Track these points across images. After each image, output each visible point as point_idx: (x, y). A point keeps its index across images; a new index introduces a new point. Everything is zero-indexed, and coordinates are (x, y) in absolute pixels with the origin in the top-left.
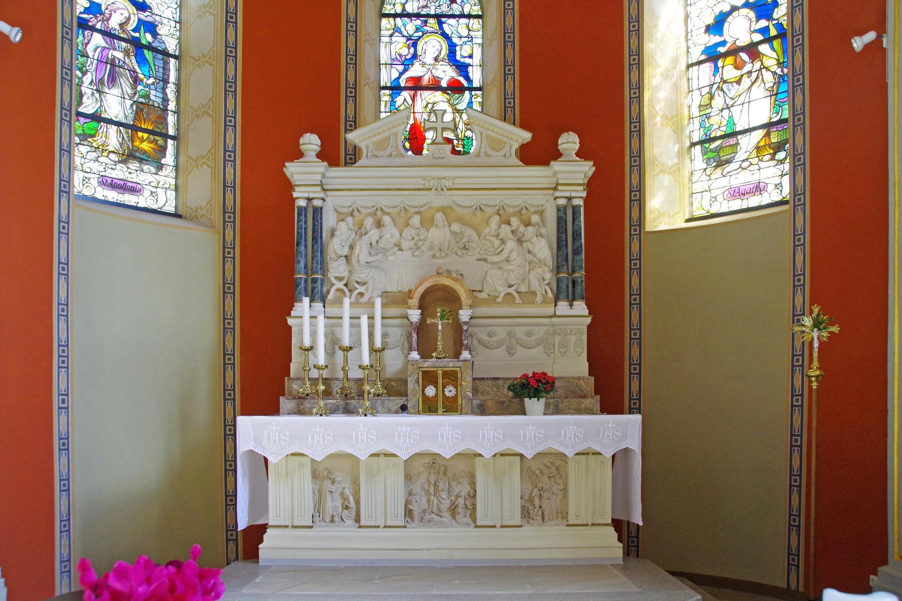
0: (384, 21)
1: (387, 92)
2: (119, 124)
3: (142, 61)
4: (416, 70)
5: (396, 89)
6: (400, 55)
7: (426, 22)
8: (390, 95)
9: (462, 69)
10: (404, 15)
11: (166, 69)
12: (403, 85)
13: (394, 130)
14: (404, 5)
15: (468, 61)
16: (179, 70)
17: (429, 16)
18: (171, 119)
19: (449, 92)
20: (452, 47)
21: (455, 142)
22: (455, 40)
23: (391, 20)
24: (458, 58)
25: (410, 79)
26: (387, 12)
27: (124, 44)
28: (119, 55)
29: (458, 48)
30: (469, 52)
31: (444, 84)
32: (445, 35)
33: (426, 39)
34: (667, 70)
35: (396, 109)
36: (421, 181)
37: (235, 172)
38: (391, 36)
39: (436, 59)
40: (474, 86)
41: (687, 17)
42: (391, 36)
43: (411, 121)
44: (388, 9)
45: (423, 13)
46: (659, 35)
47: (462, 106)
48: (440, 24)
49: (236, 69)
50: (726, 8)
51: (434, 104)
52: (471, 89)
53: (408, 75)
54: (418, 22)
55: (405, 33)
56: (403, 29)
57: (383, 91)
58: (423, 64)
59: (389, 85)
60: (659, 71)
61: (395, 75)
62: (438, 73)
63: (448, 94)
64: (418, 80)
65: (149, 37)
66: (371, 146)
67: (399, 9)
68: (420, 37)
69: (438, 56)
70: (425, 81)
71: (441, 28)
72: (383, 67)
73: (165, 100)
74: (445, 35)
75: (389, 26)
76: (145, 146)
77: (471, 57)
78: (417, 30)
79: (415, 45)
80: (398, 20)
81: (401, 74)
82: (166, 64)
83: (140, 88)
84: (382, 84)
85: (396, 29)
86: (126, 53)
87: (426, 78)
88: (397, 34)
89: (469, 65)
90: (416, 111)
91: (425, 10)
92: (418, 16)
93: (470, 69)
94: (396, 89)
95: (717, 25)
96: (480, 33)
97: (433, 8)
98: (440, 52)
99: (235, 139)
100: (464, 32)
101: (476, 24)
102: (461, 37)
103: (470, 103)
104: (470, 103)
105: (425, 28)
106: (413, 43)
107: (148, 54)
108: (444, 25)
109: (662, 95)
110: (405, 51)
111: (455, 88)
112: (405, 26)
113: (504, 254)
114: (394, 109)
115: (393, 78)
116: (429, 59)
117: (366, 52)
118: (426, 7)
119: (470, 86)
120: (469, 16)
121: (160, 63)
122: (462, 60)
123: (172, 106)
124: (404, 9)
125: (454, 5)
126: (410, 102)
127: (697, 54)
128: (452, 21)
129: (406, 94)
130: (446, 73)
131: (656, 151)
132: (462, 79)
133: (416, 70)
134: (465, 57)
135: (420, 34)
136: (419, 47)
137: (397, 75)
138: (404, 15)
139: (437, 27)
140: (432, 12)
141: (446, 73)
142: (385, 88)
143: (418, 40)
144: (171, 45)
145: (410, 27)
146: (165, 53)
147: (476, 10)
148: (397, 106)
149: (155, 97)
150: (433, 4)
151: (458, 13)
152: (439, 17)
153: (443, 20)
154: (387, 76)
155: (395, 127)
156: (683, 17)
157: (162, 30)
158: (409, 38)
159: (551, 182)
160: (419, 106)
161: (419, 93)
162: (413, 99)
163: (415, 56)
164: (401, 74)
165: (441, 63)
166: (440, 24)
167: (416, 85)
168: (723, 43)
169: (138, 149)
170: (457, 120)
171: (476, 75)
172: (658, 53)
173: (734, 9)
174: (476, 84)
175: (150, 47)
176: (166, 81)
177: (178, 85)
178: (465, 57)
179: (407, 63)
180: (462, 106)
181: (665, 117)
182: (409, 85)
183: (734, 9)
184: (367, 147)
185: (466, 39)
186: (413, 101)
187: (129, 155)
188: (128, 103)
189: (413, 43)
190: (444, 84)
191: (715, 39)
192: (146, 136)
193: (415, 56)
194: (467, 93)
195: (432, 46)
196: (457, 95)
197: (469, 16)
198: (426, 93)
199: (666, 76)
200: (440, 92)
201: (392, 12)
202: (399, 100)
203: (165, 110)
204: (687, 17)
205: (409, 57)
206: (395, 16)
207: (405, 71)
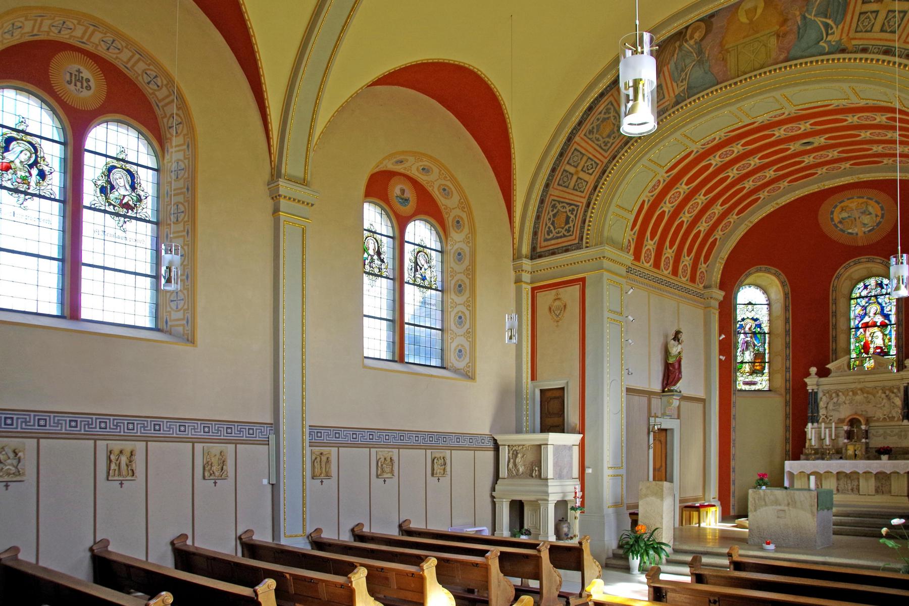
0: (852, 302)
3: (756, 338)
4: (866, 319)
5: (857, 328)
7: (870, 299)
9: (887, 316)
10: (861, 297)
11: (765, 339)
12: (860, 326)
15: (889, 313)
17: (871, 296)
18: (767, 356)
20: (882, 308)
22: (884, 305)
23: (855, 300)
24: (885, 312)
27: (750, 335)
28: (749, 339)
31: (878, 324)
39: (875, 314)
43: (864, 341)
52: (891, 325)
53: (862, 322)
54: (867, 299)
58: (870, 317)
61: (857, 322)
64: (867, 323)
65: (759, 329)
72: (852, 321)
73: (765, 350)
77: (891, 311)
78: (867, 303)
79: (865, 309)
81: (859, 322)
82: (765, 337)
83: (756, 348)
84: (851, 327)
85: (857, 304)
86: (751, 337)
93: (890, 316)
94: (857, 328)
103: (891, 331)
104: (891, 331)
106: (864, 308)
107: (759, 336)
110: (861, 313)
111: (883, 326)
113: (883, 404)
116: (871, 314)
118: (870, 292)
121: (763, 337)
123: (767, 351)
124: (860, 295)
126: (863, 333)
129: (861, 330)
130: (879, 319)
133: (866, 319)
135: (867, 304)
136: (868, 310)
138: (861, 297)
139: (875, 300)
141: (879, 319)
144: (766, 330)
145: (863, 302)
146: (765, 333)
149: (761, 349)
157: (763, 326)
158: (863, 307)
159: (900, 377)
160: (868, 333)
163: (866, 314)
164: (859, 322)
167: (866, 326)
174: (893, 322)
175: (759, 333)
176: (765, 343)
177: (769, 343)
179: (862, 317)
180: (887, 332)
188: (752, 354)
189: (864, 308)
190: (878, 324)
194: (889, 326)
195: (873, 309)
202: (858, 333)
203: (765, 353)
206: (857, 298)
207: (861, 320)
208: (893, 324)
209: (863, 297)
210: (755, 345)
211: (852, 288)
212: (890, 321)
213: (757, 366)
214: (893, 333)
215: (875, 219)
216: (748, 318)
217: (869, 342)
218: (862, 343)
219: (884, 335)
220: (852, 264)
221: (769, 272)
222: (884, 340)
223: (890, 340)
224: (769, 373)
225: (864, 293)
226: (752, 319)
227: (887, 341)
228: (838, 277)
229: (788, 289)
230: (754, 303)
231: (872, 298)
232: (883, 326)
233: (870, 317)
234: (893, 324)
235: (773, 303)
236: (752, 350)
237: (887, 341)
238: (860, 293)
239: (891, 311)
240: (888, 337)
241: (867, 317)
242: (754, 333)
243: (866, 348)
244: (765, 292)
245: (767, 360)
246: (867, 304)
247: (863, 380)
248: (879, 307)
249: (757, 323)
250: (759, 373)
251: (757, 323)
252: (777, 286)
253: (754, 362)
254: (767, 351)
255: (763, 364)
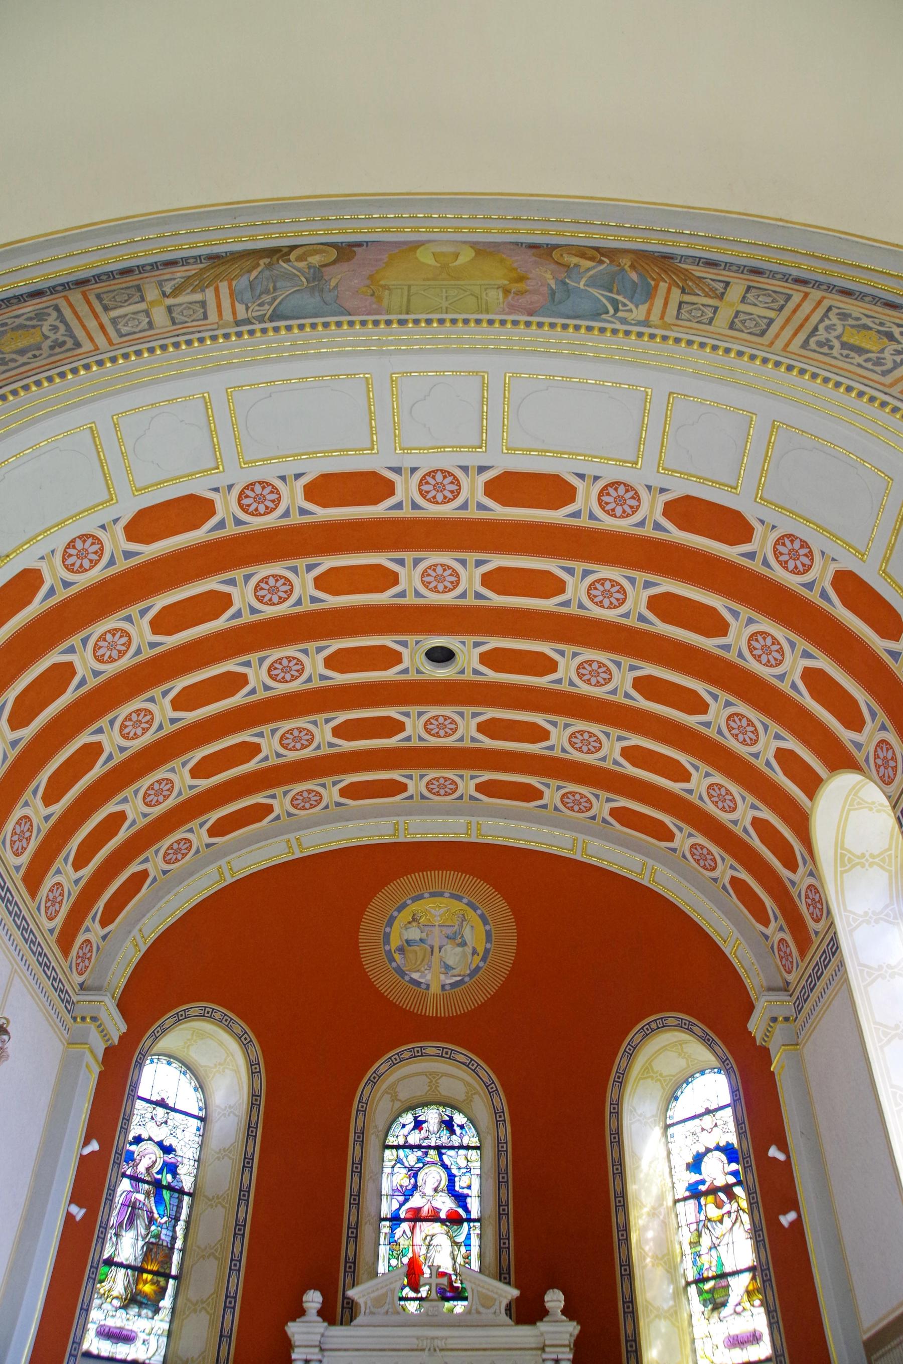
0: (388, 1153)
1: (387, 1223)
2: (127, 1267)
3: (159, 1200)
4: (416, 1201)
5: (395, 1219)
6: (401, 1186)
7: (426, 1154)
8: (390, 1227)
9: (461, 1199)
11: (179, 1207)
12: (402, 1216)
13: (392, 1286)
14: (406, 1136)
15: (466, 1191)
16: (191, 1207)
17: (429, 1147)
18: (176, 1258)
19: (448, 1223)
20: (451, 1178)
21: (454, 1277)
22: (454, 1171)
23: (394, 1151)
24: (457, 1188)
25: (410, 1210)
26: (390, 1144)
29: (457, 1179)
30: (468, 1183)
31: (443, 1215)
32: (445, 1166)
33: (426, 1170)
34: (654, 1208)
35: (396, 1242)
36: (415, 1341)
37: (233, 1320)
38: (393, 1167)
39: (436, 1190)
40: (472, 1217)
41: (669, 1154)
42: (393, 1167)
43: (410, 1255)
44: (391, 1140)
45: (424, 1144)
46: (642, 1176)
47: (461, 1239)
48: (440, 1155)
49: (247, 1213)
50: (702, 1150)
51: (433, 1236)
52: (469, 1220)
54: (419, 1153)
55: (407, 1164)
56: (404, 1160)
57: (383, 1223)
58: (424, 1195)
59: (389, 1216)
60: (645, 1210)
61: (395, 1205)
62: (437, 1204)
63: (447, 1226)
64: (418, 1210)
65: (169, 1177)
66: (369, 1302)
67: (402, 1142)
68: (420, 1168)
69: (438, 1187)
70: (424, 1212)
71: (441, 1160)
72: (384, 1199)
73: (174, 1238)
74: (445, 1166)
75: (391, 1158)
76: (148, 1288)
77: (469, 1187)
78: (419, 1160)
79: (415, 1176)
80: (401, 1151)
81: (401, 1205)
82: (181, 1201)
83: (153, 1228)
84: (383, 1215)
85: (399, 1161)
87: (425, 1209)
88: (399, 1165)
89: (468, 1196)
90: (415, 1243)
91: (426, 1141)
92: (419, 1147)
93: (468, 1200)
94: (395, 1219)
95: (696, 1165)
96: (479, 1164)
97: (434, 1140)
98: (440, 1183)
99: (237, 1284)
100: (463, 1163)
101: (474, 1155)
102: (460, 1168)
103: (469, 1234)
104: (469, 1234)
105: (426, 1159)
106: (414, 1173)
107: (166, 1194)
108: (444, 1157)
109: (650, 1234)
110: (406, 1182)
111: (454, 1220)
112: (407, 1157)
114: (393, 1242)
115: (394, 1209)
116: (429, 1190)
117: (369, 1187)
118: (427, 1138)
119: (468, 1217)
120: (468, 1148)
121: (175, 1202)
122: (461, 1191)
123: (179, 1244)
124: (406, 1141)
125: (454, 1137)
126: (409, 1233)
127: (682, 1192)
128: (452, 1153)
129: (405, 1226)
130: (445, 1204)
131: (649, 1295)
132: (461, 1211)
133: (416, 1201)
134: (464, 1188)
135: (420, 1165)
137: (397, 1206)
139: (437, 1158)
140: (433, 1144)
142: (385, 1219)
143: (419, 1171)
144: (187, 1183)
145: (412, 1158)
146: (181, 1192)
147: (475, 1142)
148: (396, 1238)
149: (165, 1235)
150: (434, 1135)
151: (457, 1144)
152: (439, 1148)
153: (443, 1151)
154: (387, 1207)
155: (391, 1283)
156: (665, 1153)
157: (181, 1170)
160: (419, 1238)
161: (418, 1224)
162: (412, 1230)
164: (401, 1205)
165: (440, 1194)
166: (440, 1155)
167: (416, 1217)
168: (703, 1182)
169: (140, 1292)
170: (456, 1253)
171: (474, 1205)
172: (643, 1193)
173: (708, 1150)
174: (474, 1215)
175: (169, 1187)
176: (177, 1219)
177: (188, 1223)
178: (464, 1188)
179: (408, 1194)
181: (655, 1257)
182: (409, 1216)
183: (708, 1150)
184: (366, 1303)
185: (465, 1170)
186: (412, 1233)
187: (133, 1300)
188: (141, 1243)
189: (414, 1173)
190: (443, 1215)
191: (695, 1177)
192: (150, 1277)
193: (415, 1187)
194: (465, 1224)
195: (432, 1177)
196: (455, 1227)
197: (468, 1148)
198: (425, 1225)
199: (653, 1214)
200: (439, 1224)
201: (395, 1143)
202: (398, 1232)
203: (172, 1249)
204: (669, 1154)
205: (410, 1187)
206: (398, 1147)
207: (406, 1201)
208: (475, 1220)
209: (412, 1147)
210: (151, 1220)
211: (392, 1118)
212: (468, 1211)
213: (146, 1282)
214: (475, 1242)
215: (470, 956)
216: (150, 1139)
217: (422, 1259)
218: (405, 1260)
219: (455, 1244)
220: (407, 1055)
221: (229, 1029)
222: (454, 1259)
223: (467, 1257)
224: (173, 1310)
225: (414, 1139)
226: (160, 1144)
227: (460, 1260)
228: (373, 1082)
229: (262, 1083)
230: (171, 1105)
231: (432, 1152)
232: (454, 1220)
233: (424, 1195)
234: (475, 1220)
235: (215, 1115)
236: (143, 1231)
237: (460, 1260)
238: (406, 1136)
239: (469, 1187)
240: (463, 1249)
241: (417, 1195)
242: (157, 1185)
243: (413, 1272)
244: (201, 1086)
245: (174, 1272)
246: (420, 1165)
247: (439, 1343)
248: (444, 1177)
249: (169, 1158)
250: (146, 1306)
251: (169, 1158)
252: (237, 1072)
253: (141, 1270)
254: (179, 1244)
255: (162, 1280)
